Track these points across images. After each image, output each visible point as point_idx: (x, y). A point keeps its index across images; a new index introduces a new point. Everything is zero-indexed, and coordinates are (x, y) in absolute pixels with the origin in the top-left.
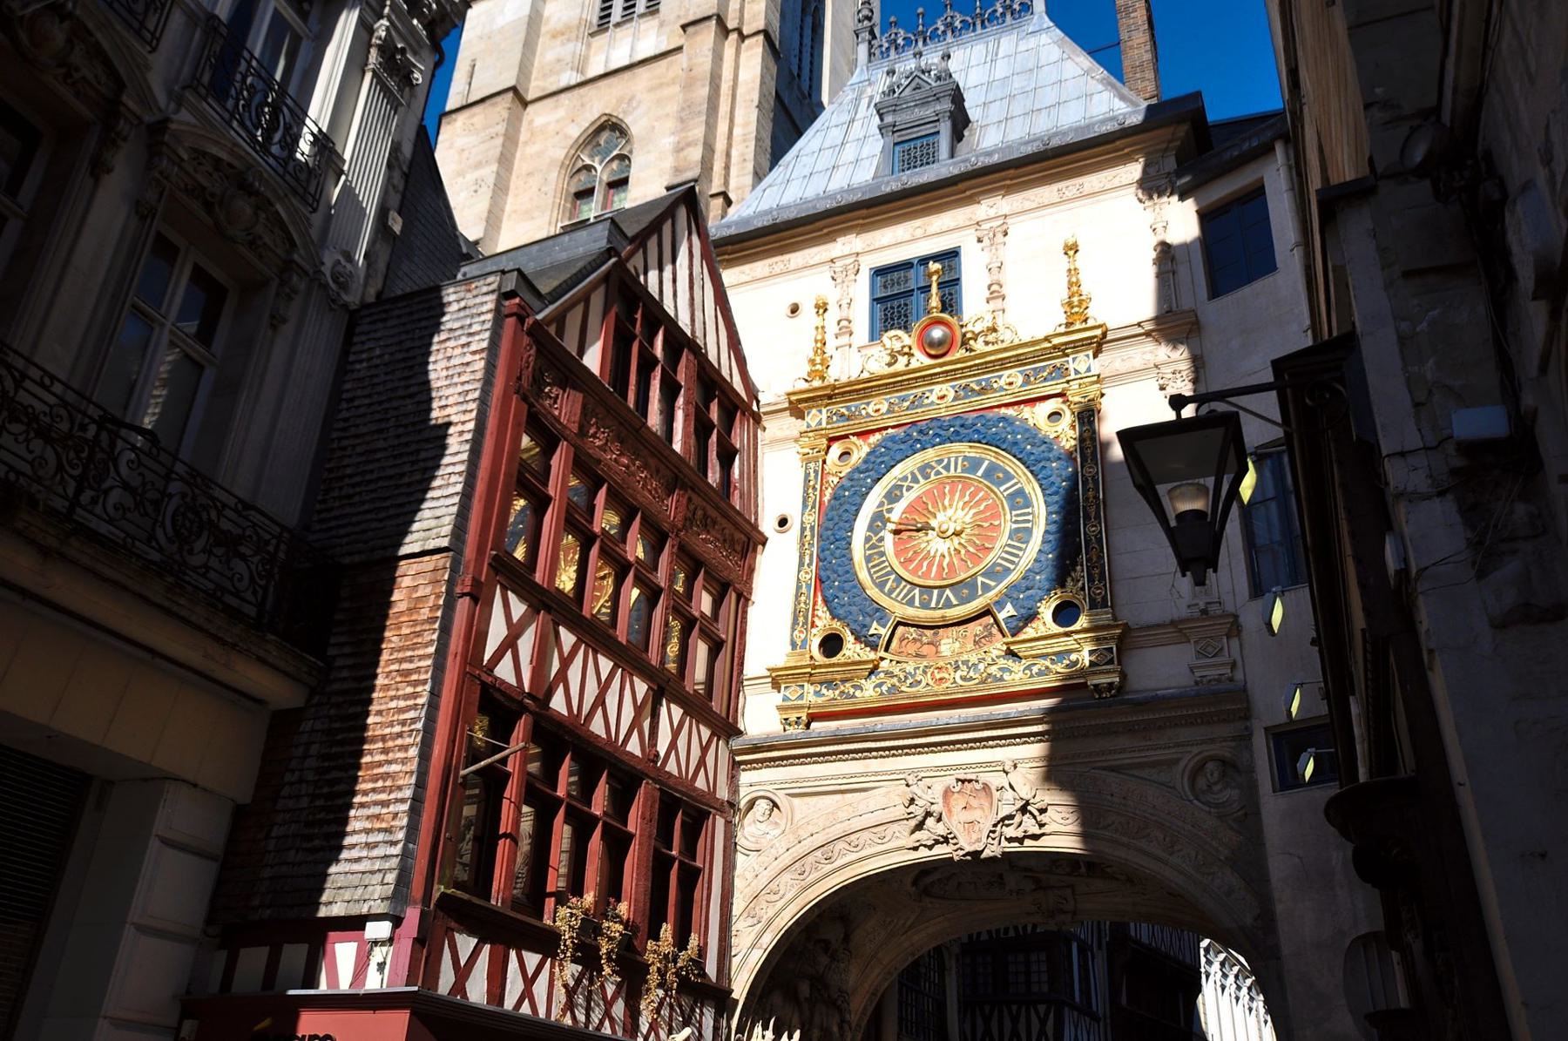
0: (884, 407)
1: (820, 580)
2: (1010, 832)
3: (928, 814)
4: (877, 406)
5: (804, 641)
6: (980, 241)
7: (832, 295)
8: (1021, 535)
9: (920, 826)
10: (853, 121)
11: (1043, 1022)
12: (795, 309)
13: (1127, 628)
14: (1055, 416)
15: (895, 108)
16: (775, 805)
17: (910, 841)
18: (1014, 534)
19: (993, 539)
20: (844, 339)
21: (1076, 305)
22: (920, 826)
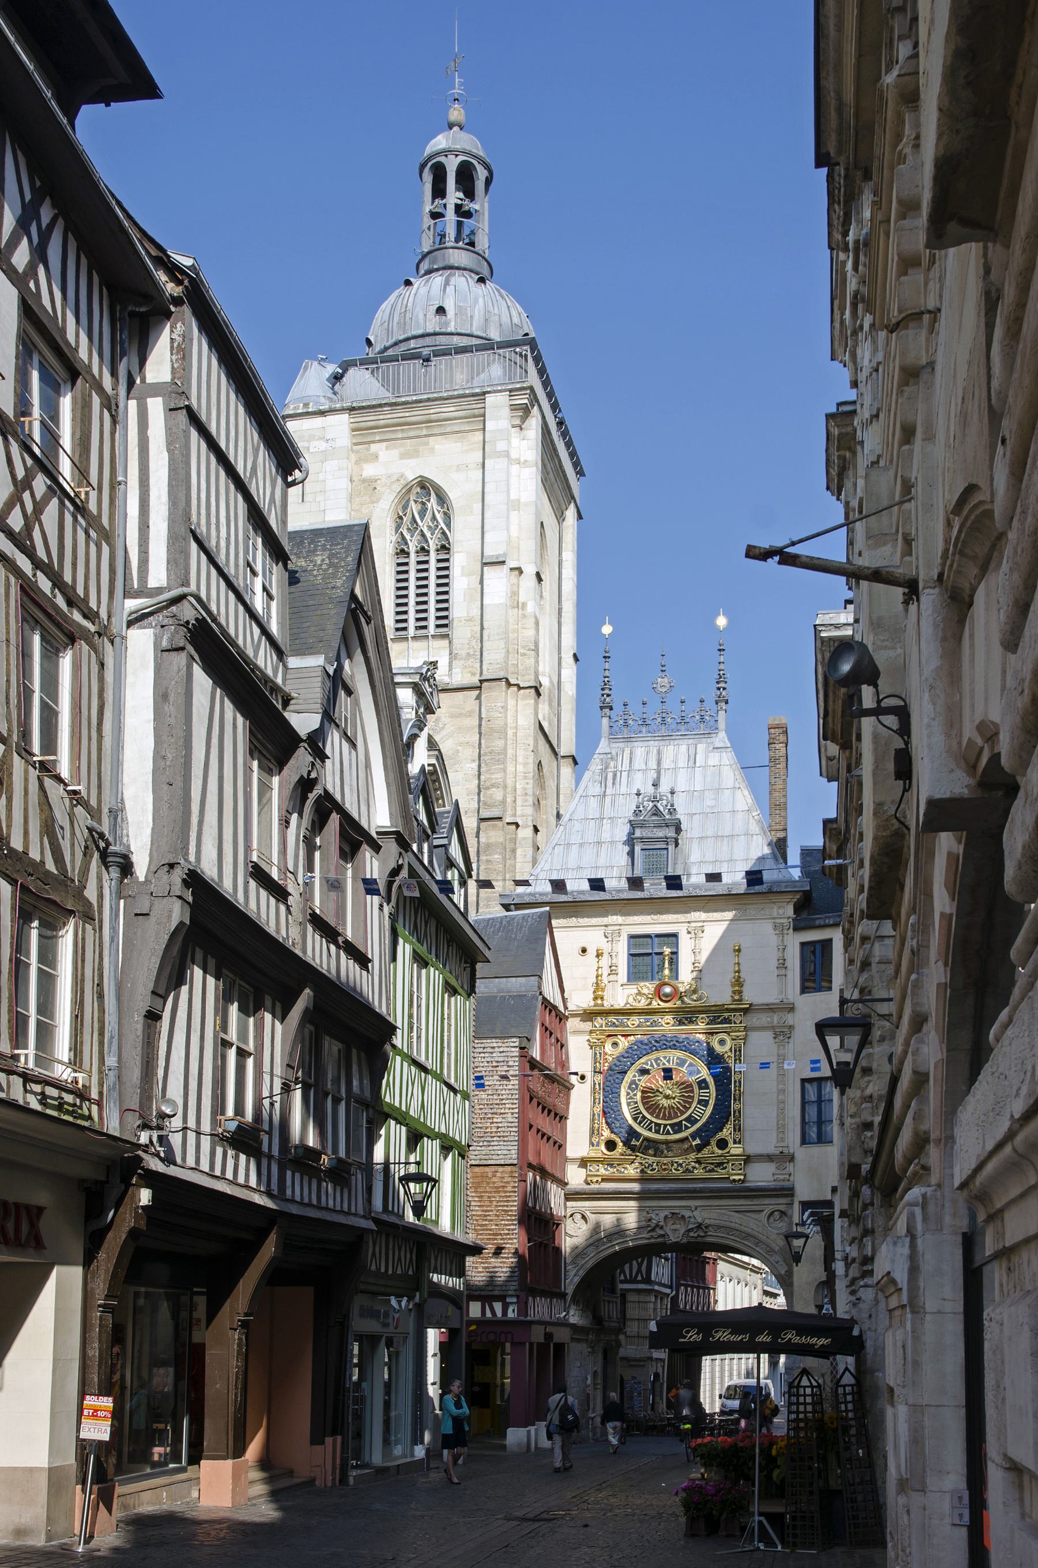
0: (637, 1023)
1: (604, 1112)
2: (691, 1234)
3: (657, 1226)
4: (635, 1020)
5: (598, 1143)
6: (689, 933)
7: (606, 947)
8: (704, 1103)
9: (653, 1230)
10: (604, 795)
11: (640, 1265)
12: (584, 950)
13: (749, 1156)
14: (722, 1042)
15: (642, 825)
16: (584, 1217)
17: (648, 1236)
18: (700, 1102)
19: (691, 1103)
20: (612, 978)
21: (738, 982)
22: (653, 1230)
